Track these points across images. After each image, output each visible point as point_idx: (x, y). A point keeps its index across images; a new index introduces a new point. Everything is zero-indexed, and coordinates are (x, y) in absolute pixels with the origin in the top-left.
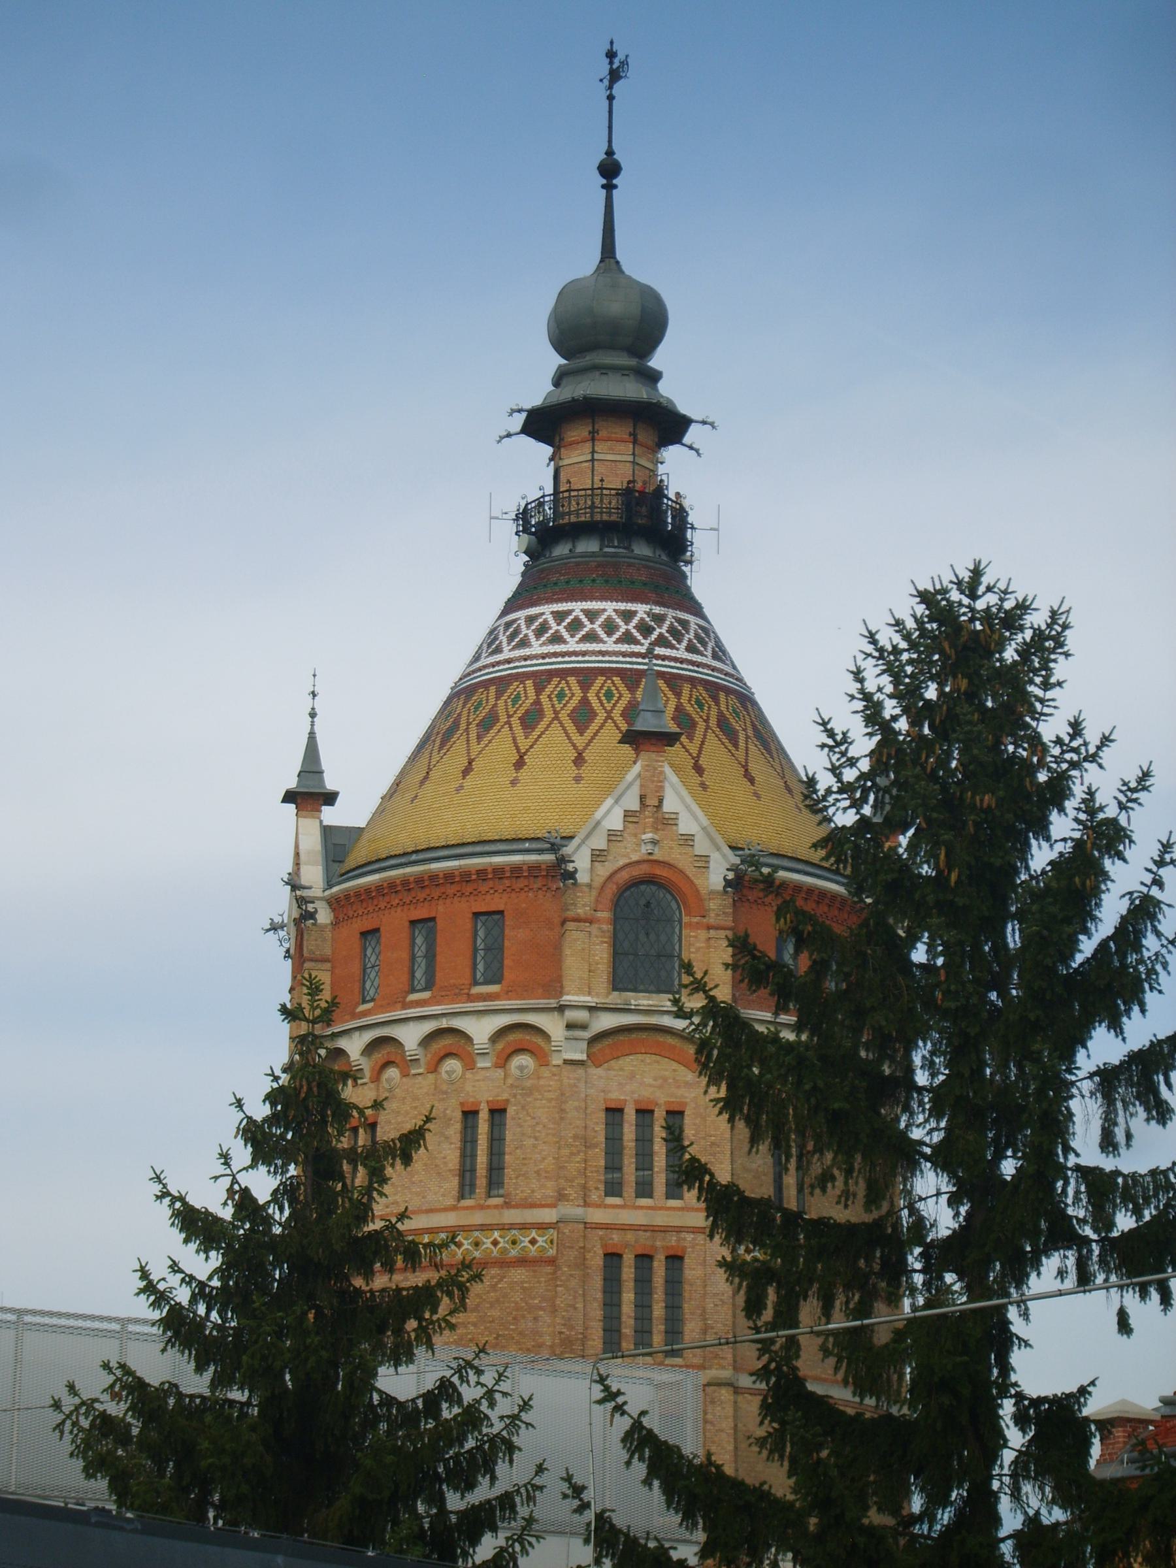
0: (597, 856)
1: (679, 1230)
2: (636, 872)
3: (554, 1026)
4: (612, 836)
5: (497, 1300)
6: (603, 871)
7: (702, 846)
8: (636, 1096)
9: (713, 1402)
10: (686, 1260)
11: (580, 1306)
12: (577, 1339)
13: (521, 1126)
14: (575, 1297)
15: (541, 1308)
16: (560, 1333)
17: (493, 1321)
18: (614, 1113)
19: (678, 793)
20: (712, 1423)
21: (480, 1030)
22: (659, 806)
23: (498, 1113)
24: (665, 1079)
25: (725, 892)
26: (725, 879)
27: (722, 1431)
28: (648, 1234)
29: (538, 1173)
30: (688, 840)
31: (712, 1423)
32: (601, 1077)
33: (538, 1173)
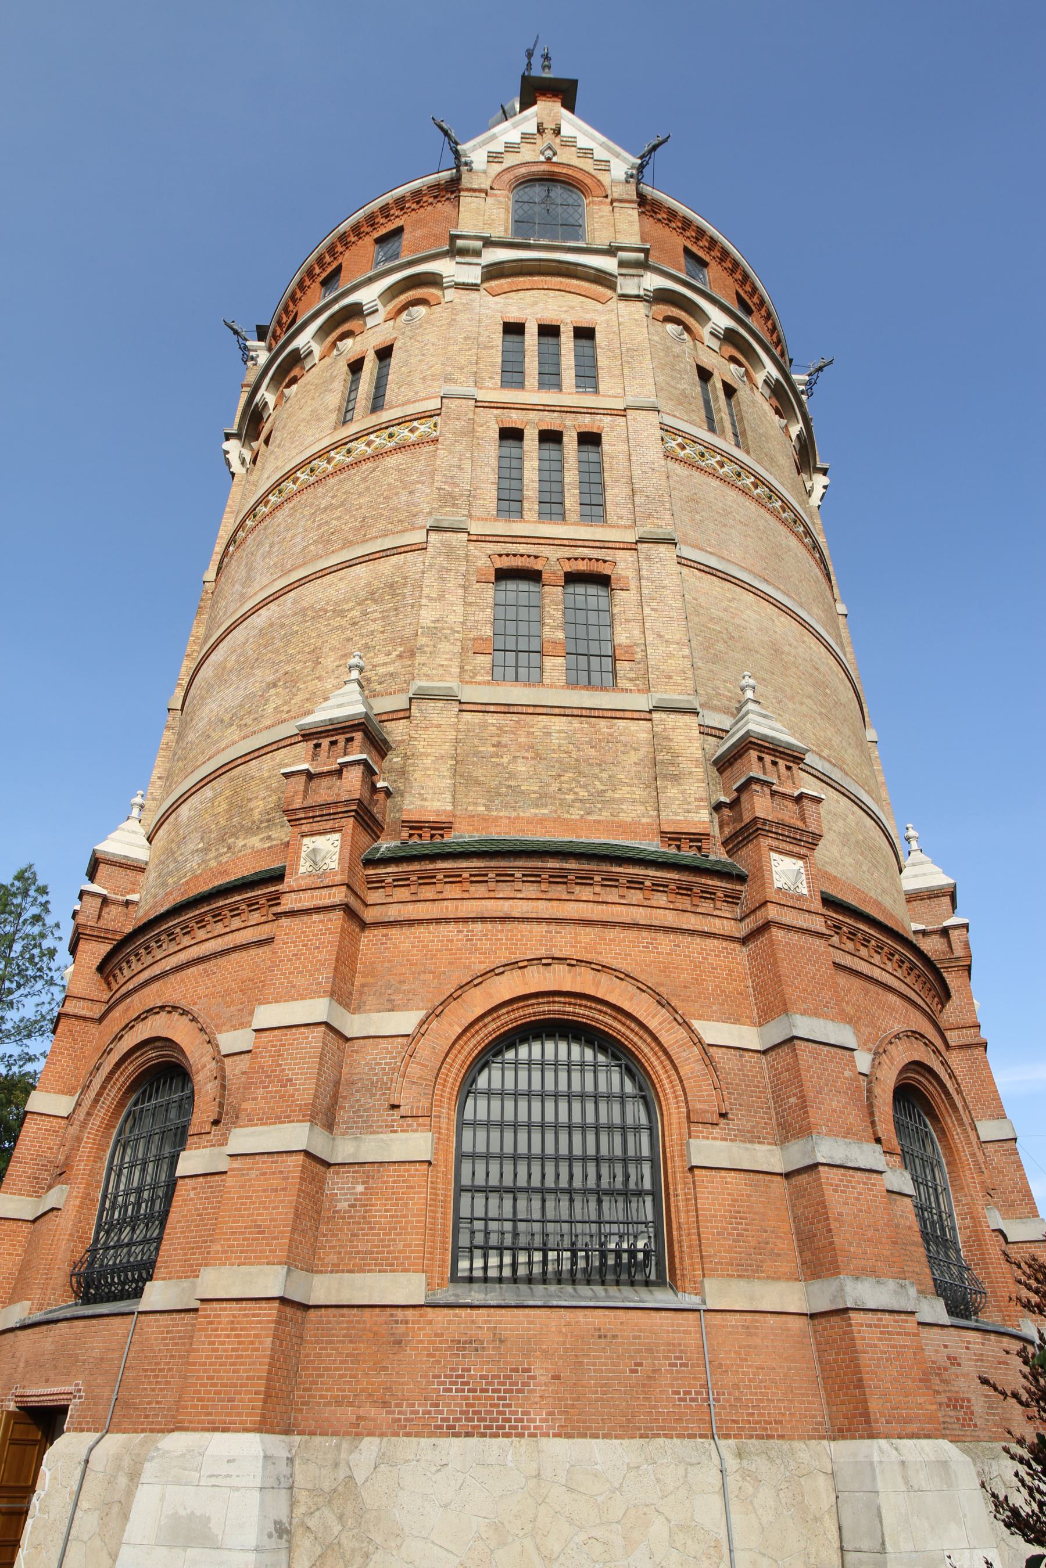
0: (494, 158)
1: (592, 412)
2: (535, 169)
3: (445, 267)
4: (510, 148)
5: (368, 488)
6: (497, 168)
7: (600, 154)
8: (539, 316)
9: (648, 559)
10: (604, 438)
11: (467, 466)
12: (462, 495)
13: (407, 351)
14: (460, 460)
15: (418, 482)
16: (439, 489)
17: (361, 508)
18: (514, 329)
19: (574, 125)
20: (648, 579)
21: (367, 296)
22: (557, 132)
23: (384, 354)
24: (572, 308)
25: (627, 182)
26: (626, 173)
27: (663, 587)
28: (556, 414)
29: (424, 379)
30: (587, 153)
31: (648, 579)
32: (497, 303)
33: (424, 379)
